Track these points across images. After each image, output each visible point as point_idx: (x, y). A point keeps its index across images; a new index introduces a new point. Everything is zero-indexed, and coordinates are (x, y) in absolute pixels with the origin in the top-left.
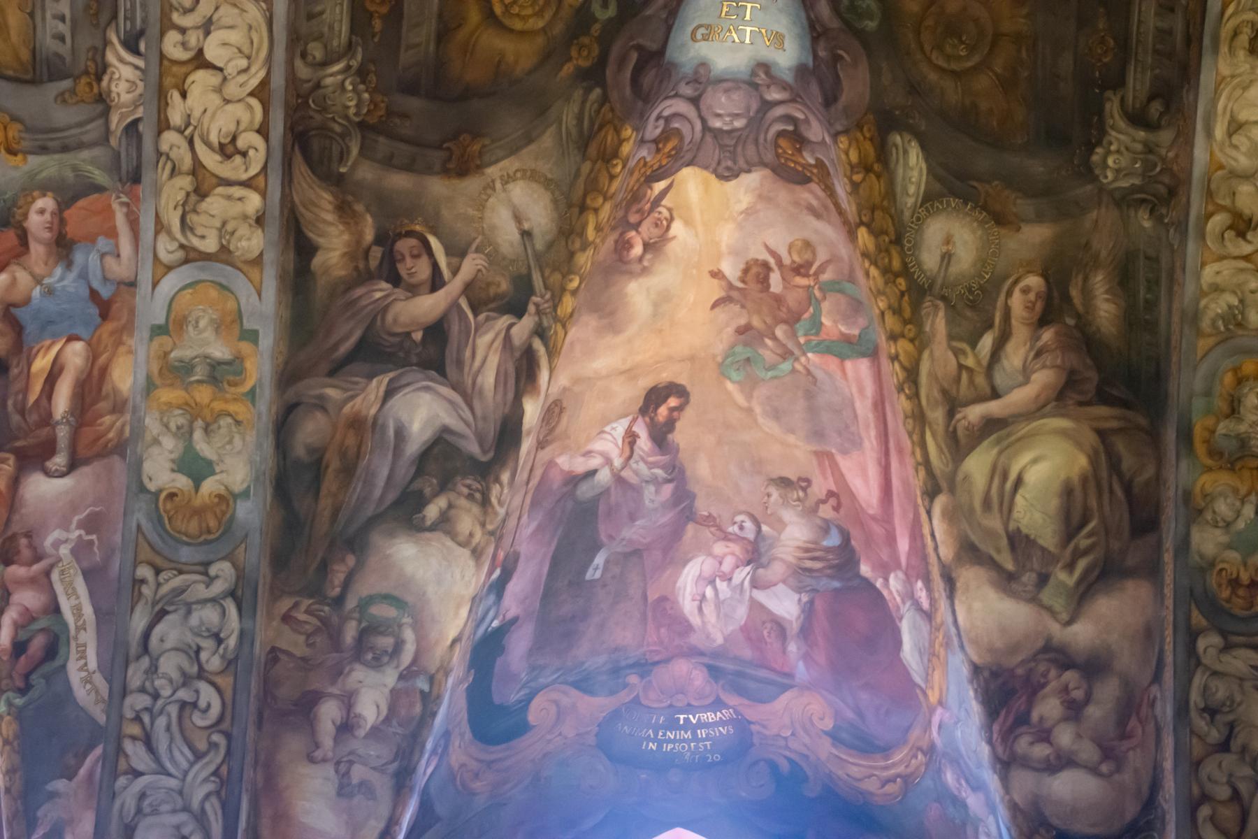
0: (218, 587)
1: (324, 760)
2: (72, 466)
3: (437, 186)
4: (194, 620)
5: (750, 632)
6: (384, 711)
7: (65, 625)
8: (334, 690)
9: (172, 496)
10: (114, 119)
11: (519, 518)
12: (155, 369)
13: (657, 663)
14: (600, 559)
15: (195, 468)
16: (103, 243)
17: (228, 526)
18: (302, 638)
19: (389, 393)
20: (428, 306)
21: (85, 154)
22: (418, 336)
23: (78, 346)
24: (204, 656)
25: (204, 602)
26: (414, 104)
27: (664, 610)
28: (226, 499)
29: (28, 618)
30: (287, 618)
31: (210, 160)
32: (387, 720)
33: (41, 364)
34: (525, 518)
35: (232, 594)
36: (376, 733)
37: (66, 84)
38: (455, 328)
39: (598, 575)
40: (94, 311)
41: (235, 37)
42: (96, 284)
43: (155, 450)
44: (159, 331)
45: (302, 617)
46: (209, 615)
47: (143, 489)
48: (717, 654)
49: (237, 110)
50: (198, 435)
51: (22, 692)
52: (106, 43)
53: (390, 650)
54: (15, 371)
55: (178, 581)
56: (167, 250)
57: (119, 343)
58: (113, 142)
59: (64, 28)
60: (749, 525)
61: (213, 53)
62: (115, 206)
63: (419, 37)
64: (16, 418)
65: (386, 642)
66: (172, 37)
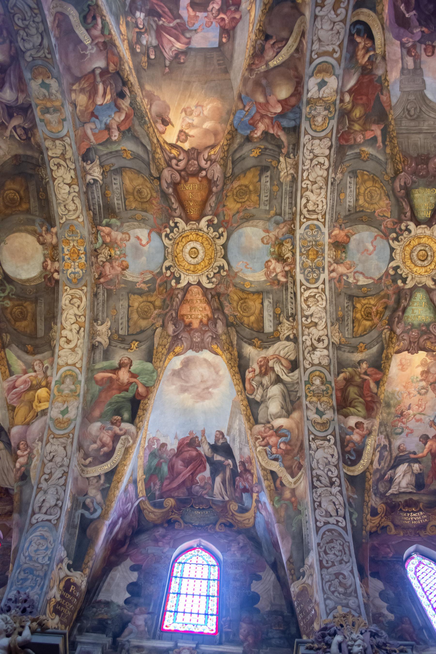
0: (28, 54)
2: (93, 71)
3: (20, 152)
4: (31, 44)
7: (83, 26)
9: (49, 78)
10: (98, 162)
12: (63, 110)
15: (44, 85)
16: (97, 131)
17: (31, 70)
19: (17, 99)
20: (15, 122)
21: (105, 152)
22: (15, 114)
23: (99, 103)
24: (25, 34)
25: (30, 50)
26: (30, 172)
28: (34, 78)
29: (95, 26)
31: (62, 162)
33: (108, 97)
35: (24, 53)
37: (112, 169)
38: (7, 117)
40: (96, 113)
41: (63, 191)
42: (97, 120)
43: (57, 89)
44: (64, 120)
46: (28, 46)
47: (56, 79)
49: (59, 175)
50: (47, 94)
51: (89, 6)
52: (103, 180)
54: (115, 94)
55: (39, 54)
56: (68, 140)
57: (86, 107)
58: (97, 157)
59: (114, 181)
61: (67, 187)
62: (94, 141)
63: (32, 188)
64: (112, 82)
66: (77, 190)
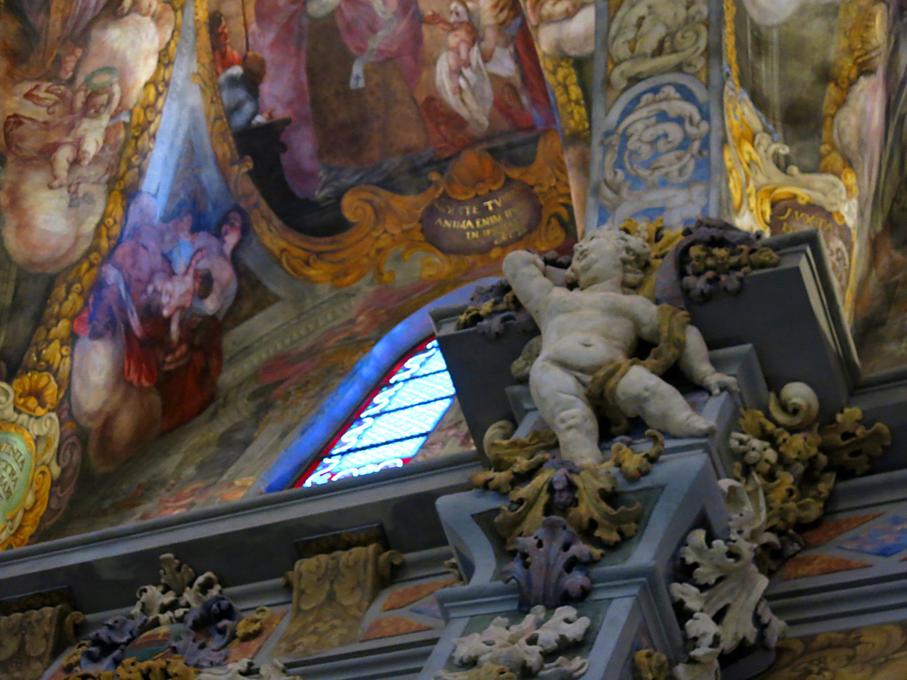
1: (61, 186)
5: (499, 105)
6: (101, 143)
8: (69, 139)
11: (246, 25)
13: (448, 159)
14: (357, 69)
18: (44, 110)
27: (434, 109)
30: (28, 96)
32: (103, 149)
34: (253, 27)
36: (96, 159)
39: (362, 84)
45: (42, 95)
48: (489, 137)
53: (105, 103)
60: (460, 9)
65: (104, 98)
